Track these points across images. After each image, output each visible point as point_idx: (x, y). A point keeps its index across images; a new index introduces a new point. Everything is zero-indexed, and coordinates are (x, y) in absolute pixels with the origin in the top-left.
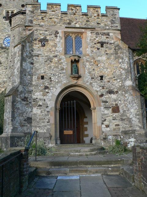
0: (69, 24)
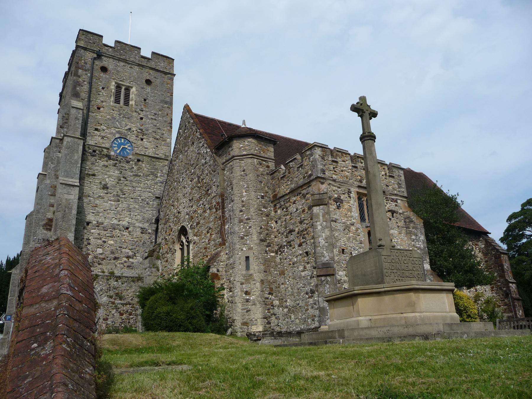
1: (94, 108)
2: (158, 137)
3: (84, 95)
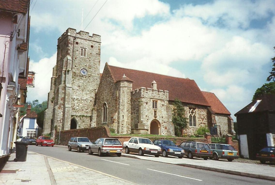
0: (154, 97)
2: (95, 67)
3: (71, 54)
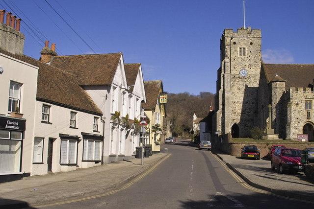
1: (232, 60)
3: (229, 56)
